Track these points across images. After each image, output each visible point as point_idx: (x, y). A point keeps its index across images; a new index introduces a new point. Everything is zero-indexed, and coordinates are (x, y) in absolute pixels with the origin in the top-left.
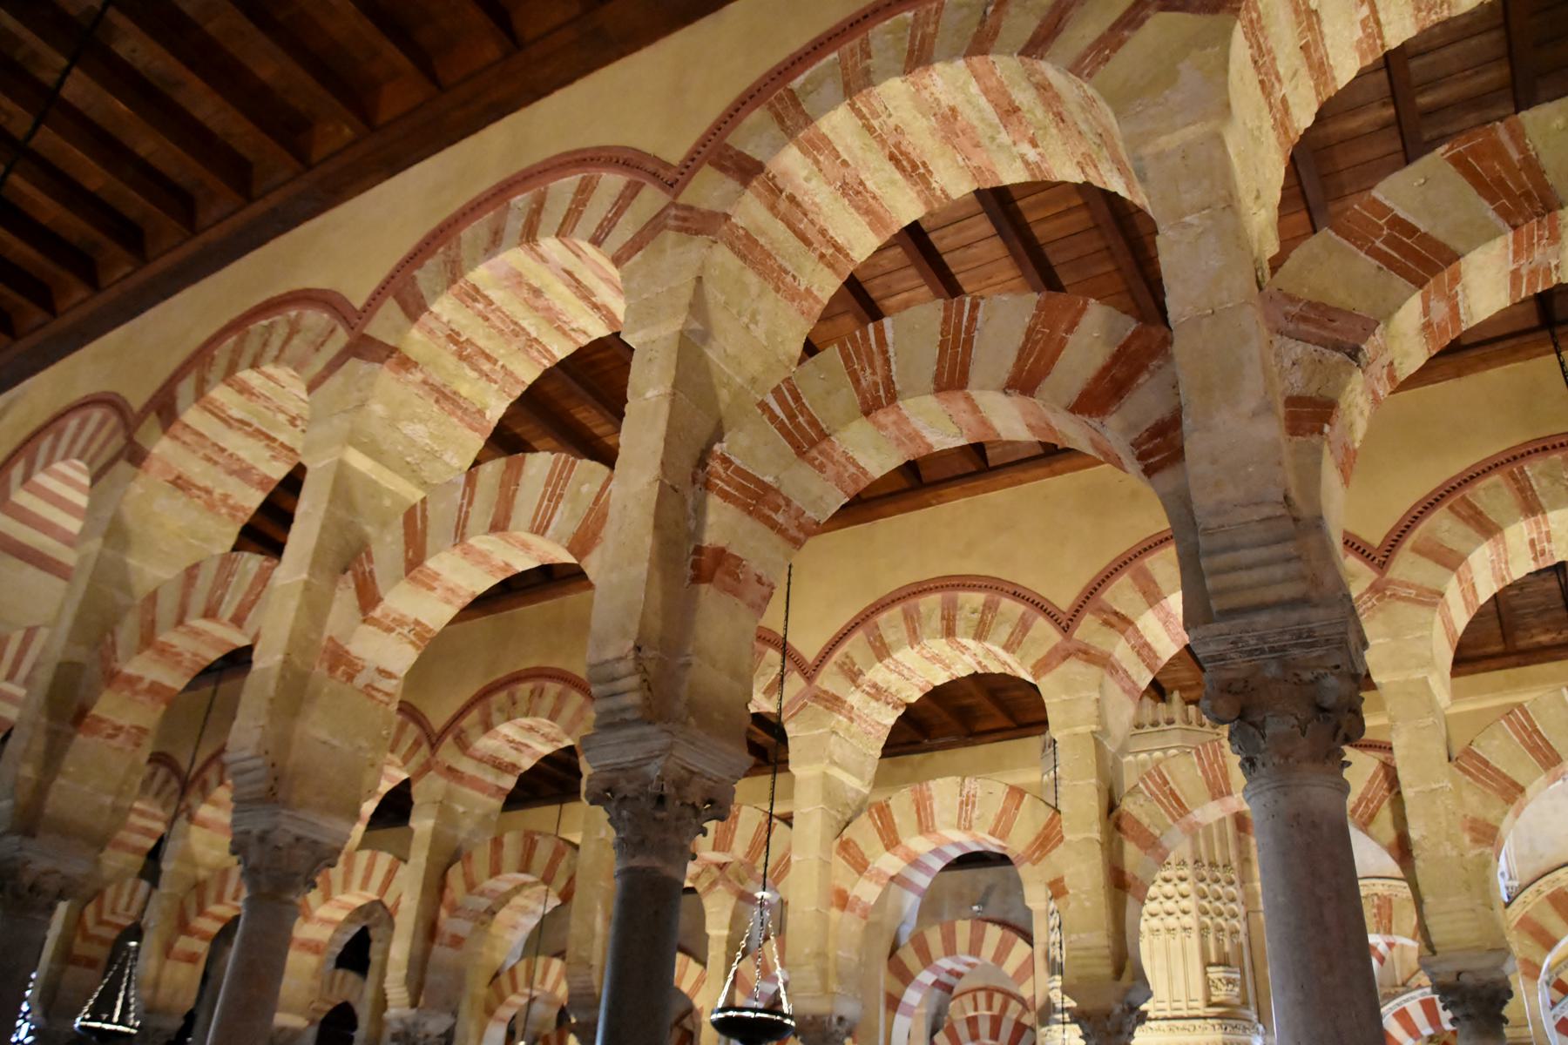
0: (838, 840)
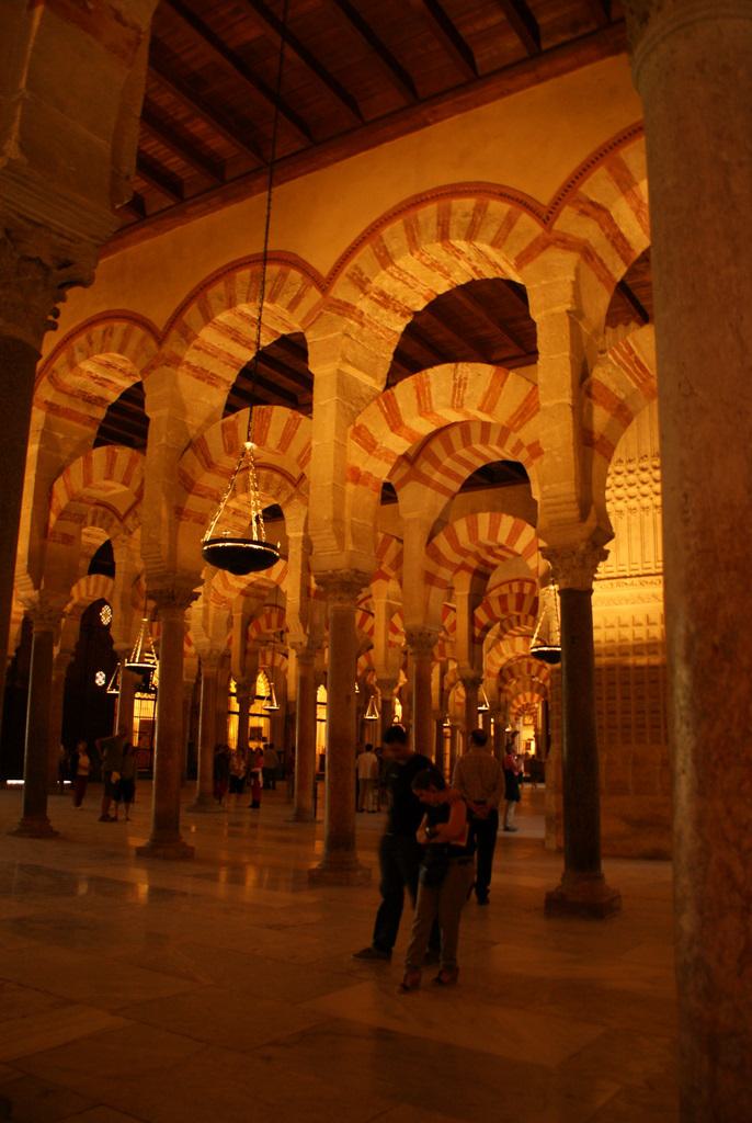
0: (352, 427)
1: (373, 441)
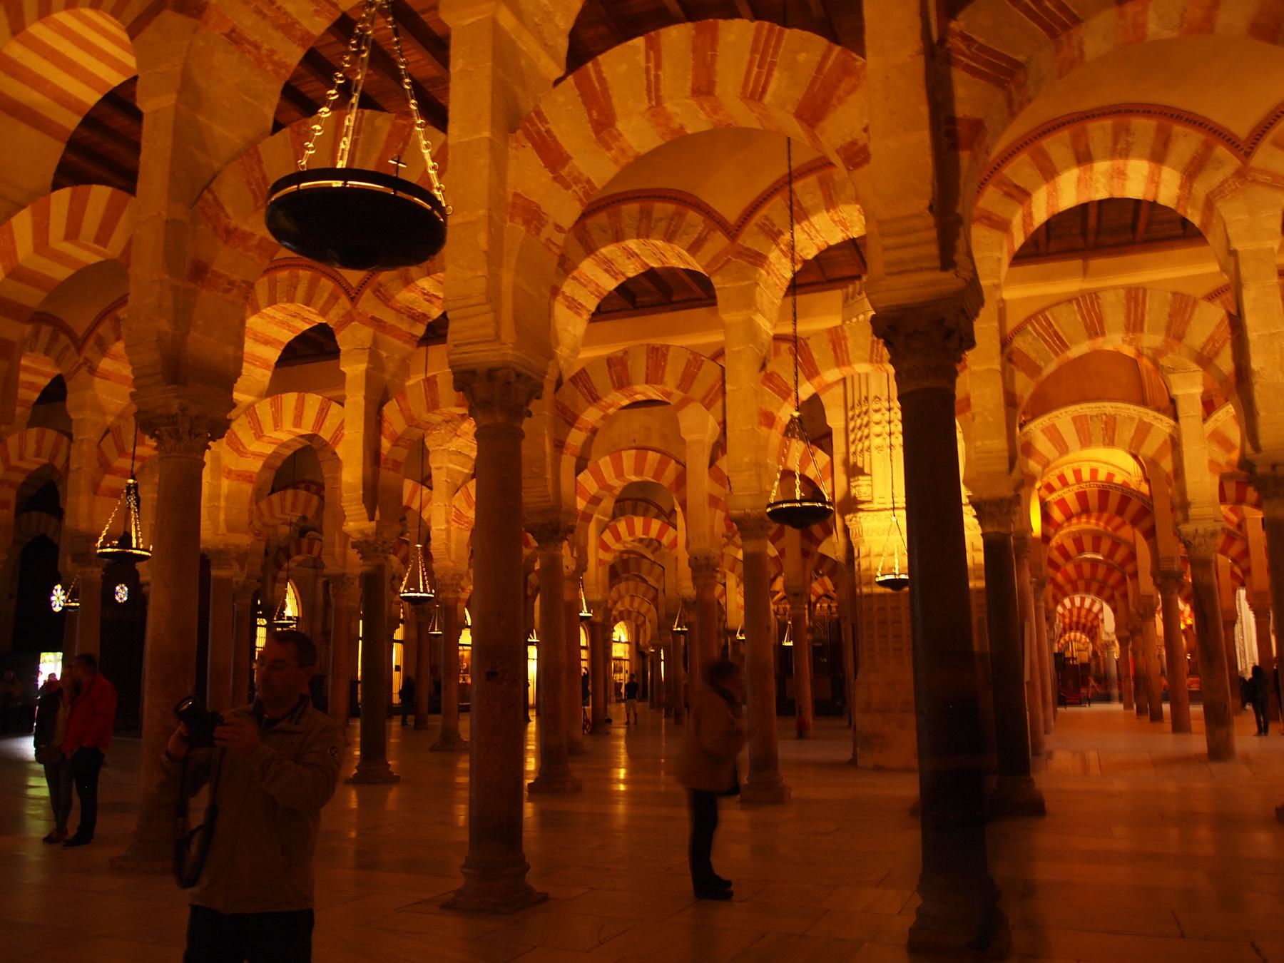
0: (763, 372)
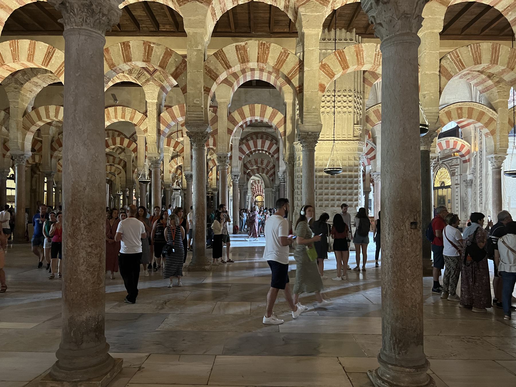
1: (333, 73)
